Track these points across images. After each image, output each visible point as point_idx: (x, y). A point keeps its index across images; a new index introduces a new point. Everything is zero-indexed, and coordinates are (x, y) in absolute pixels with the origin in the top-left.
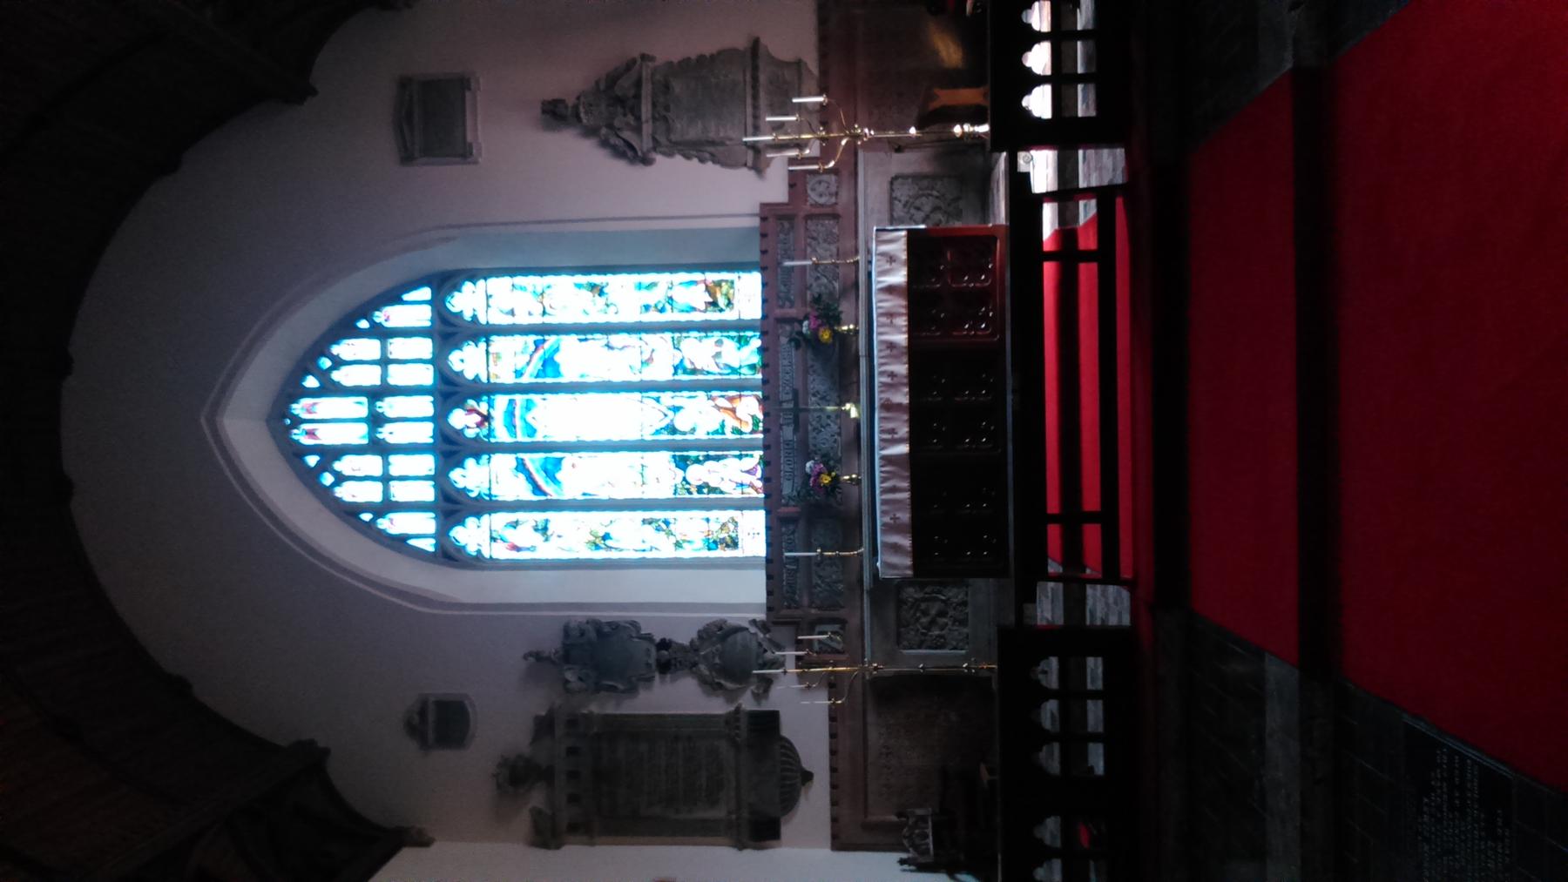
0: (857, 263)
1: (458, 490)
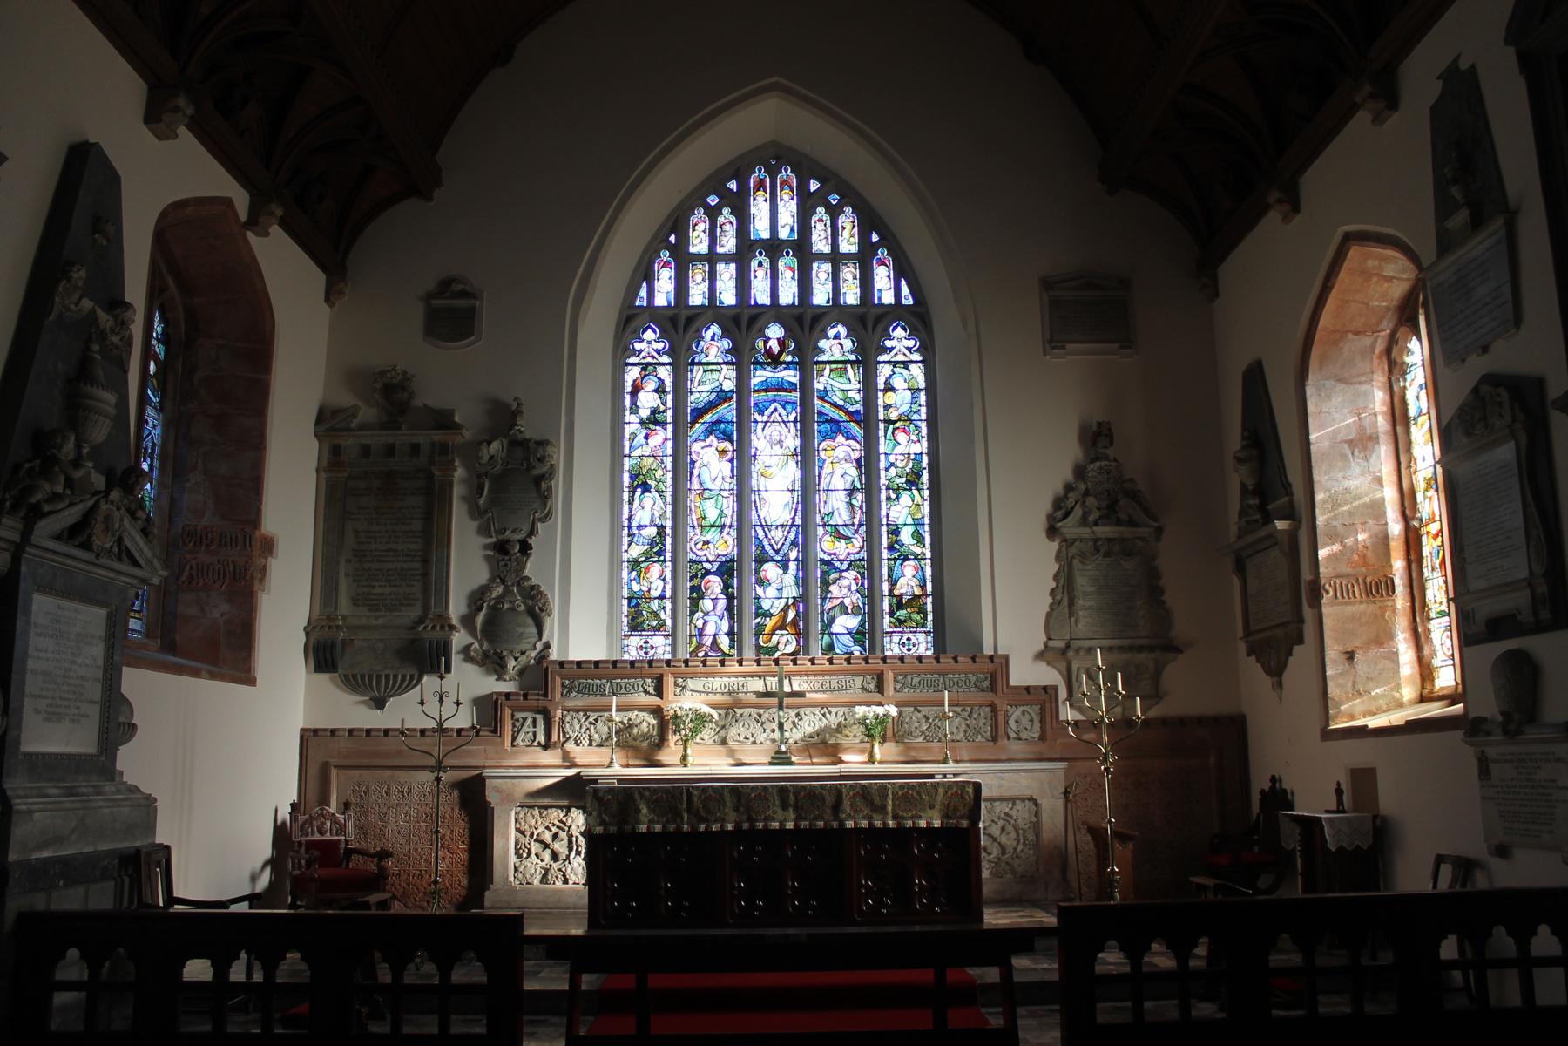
0: (945, 761)
1: (699, 331)
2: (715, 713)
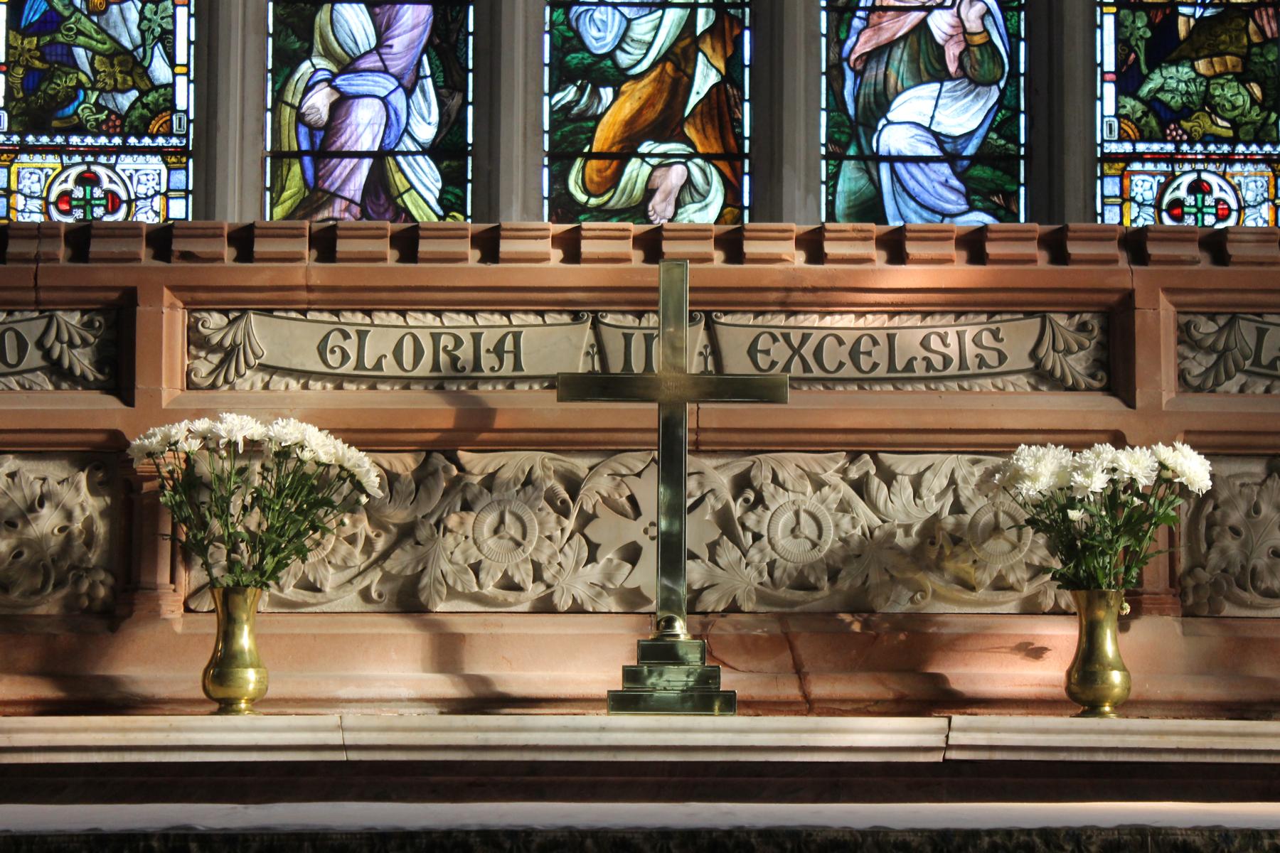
2: (367, 468)
